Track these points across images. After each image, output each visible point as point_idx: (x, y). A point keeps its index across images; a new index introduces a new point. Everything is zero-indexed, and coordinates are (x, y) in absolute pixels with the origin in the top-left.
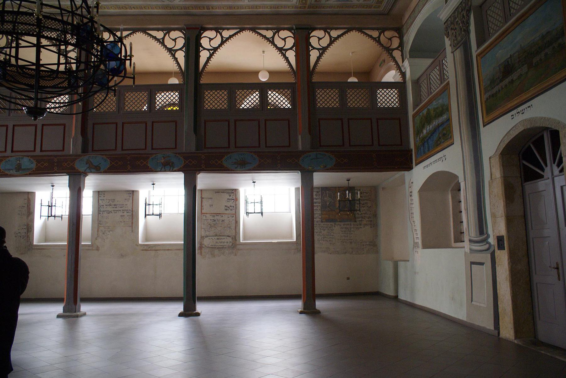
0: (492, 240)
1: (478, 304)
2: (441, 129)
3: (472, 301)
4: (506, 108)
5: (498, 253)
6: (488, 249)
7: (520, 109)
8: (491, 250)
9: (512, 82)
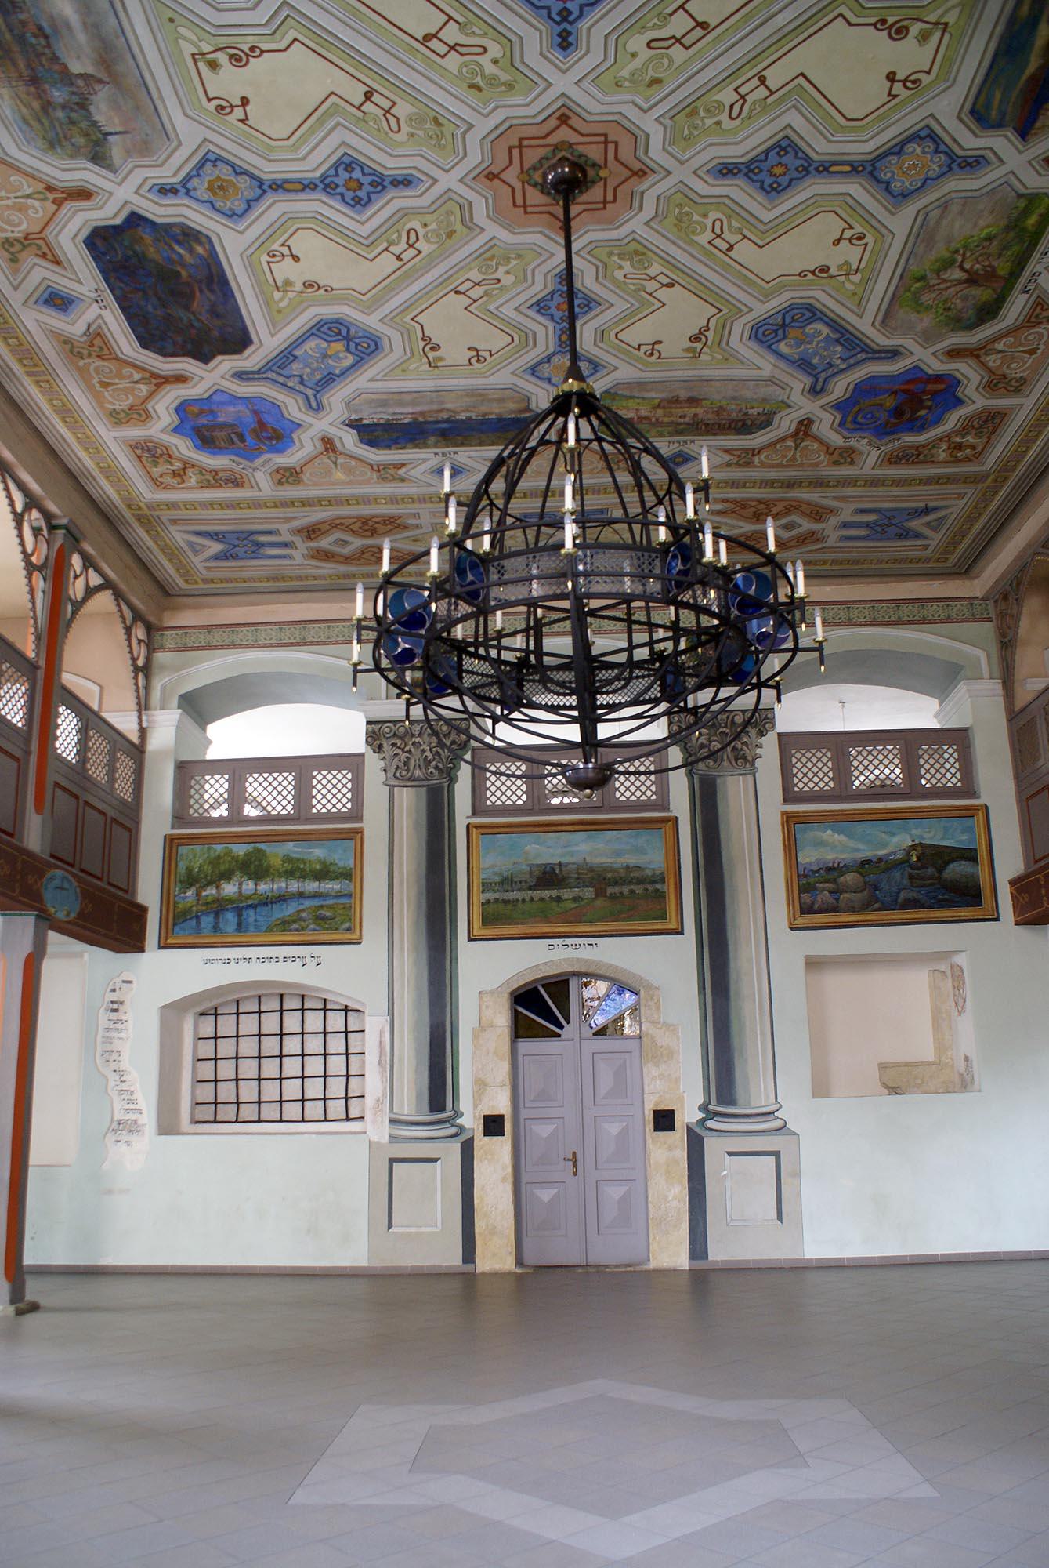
0: (470, 1120)
1: (413, 1230)
2: (308, 903)
3: (390, 1226)
4: (533, 930)
5: (482, 1142)
6: (456, 1135)
7: (568, 941)
8: (464, 1137)
9: (559, 899)
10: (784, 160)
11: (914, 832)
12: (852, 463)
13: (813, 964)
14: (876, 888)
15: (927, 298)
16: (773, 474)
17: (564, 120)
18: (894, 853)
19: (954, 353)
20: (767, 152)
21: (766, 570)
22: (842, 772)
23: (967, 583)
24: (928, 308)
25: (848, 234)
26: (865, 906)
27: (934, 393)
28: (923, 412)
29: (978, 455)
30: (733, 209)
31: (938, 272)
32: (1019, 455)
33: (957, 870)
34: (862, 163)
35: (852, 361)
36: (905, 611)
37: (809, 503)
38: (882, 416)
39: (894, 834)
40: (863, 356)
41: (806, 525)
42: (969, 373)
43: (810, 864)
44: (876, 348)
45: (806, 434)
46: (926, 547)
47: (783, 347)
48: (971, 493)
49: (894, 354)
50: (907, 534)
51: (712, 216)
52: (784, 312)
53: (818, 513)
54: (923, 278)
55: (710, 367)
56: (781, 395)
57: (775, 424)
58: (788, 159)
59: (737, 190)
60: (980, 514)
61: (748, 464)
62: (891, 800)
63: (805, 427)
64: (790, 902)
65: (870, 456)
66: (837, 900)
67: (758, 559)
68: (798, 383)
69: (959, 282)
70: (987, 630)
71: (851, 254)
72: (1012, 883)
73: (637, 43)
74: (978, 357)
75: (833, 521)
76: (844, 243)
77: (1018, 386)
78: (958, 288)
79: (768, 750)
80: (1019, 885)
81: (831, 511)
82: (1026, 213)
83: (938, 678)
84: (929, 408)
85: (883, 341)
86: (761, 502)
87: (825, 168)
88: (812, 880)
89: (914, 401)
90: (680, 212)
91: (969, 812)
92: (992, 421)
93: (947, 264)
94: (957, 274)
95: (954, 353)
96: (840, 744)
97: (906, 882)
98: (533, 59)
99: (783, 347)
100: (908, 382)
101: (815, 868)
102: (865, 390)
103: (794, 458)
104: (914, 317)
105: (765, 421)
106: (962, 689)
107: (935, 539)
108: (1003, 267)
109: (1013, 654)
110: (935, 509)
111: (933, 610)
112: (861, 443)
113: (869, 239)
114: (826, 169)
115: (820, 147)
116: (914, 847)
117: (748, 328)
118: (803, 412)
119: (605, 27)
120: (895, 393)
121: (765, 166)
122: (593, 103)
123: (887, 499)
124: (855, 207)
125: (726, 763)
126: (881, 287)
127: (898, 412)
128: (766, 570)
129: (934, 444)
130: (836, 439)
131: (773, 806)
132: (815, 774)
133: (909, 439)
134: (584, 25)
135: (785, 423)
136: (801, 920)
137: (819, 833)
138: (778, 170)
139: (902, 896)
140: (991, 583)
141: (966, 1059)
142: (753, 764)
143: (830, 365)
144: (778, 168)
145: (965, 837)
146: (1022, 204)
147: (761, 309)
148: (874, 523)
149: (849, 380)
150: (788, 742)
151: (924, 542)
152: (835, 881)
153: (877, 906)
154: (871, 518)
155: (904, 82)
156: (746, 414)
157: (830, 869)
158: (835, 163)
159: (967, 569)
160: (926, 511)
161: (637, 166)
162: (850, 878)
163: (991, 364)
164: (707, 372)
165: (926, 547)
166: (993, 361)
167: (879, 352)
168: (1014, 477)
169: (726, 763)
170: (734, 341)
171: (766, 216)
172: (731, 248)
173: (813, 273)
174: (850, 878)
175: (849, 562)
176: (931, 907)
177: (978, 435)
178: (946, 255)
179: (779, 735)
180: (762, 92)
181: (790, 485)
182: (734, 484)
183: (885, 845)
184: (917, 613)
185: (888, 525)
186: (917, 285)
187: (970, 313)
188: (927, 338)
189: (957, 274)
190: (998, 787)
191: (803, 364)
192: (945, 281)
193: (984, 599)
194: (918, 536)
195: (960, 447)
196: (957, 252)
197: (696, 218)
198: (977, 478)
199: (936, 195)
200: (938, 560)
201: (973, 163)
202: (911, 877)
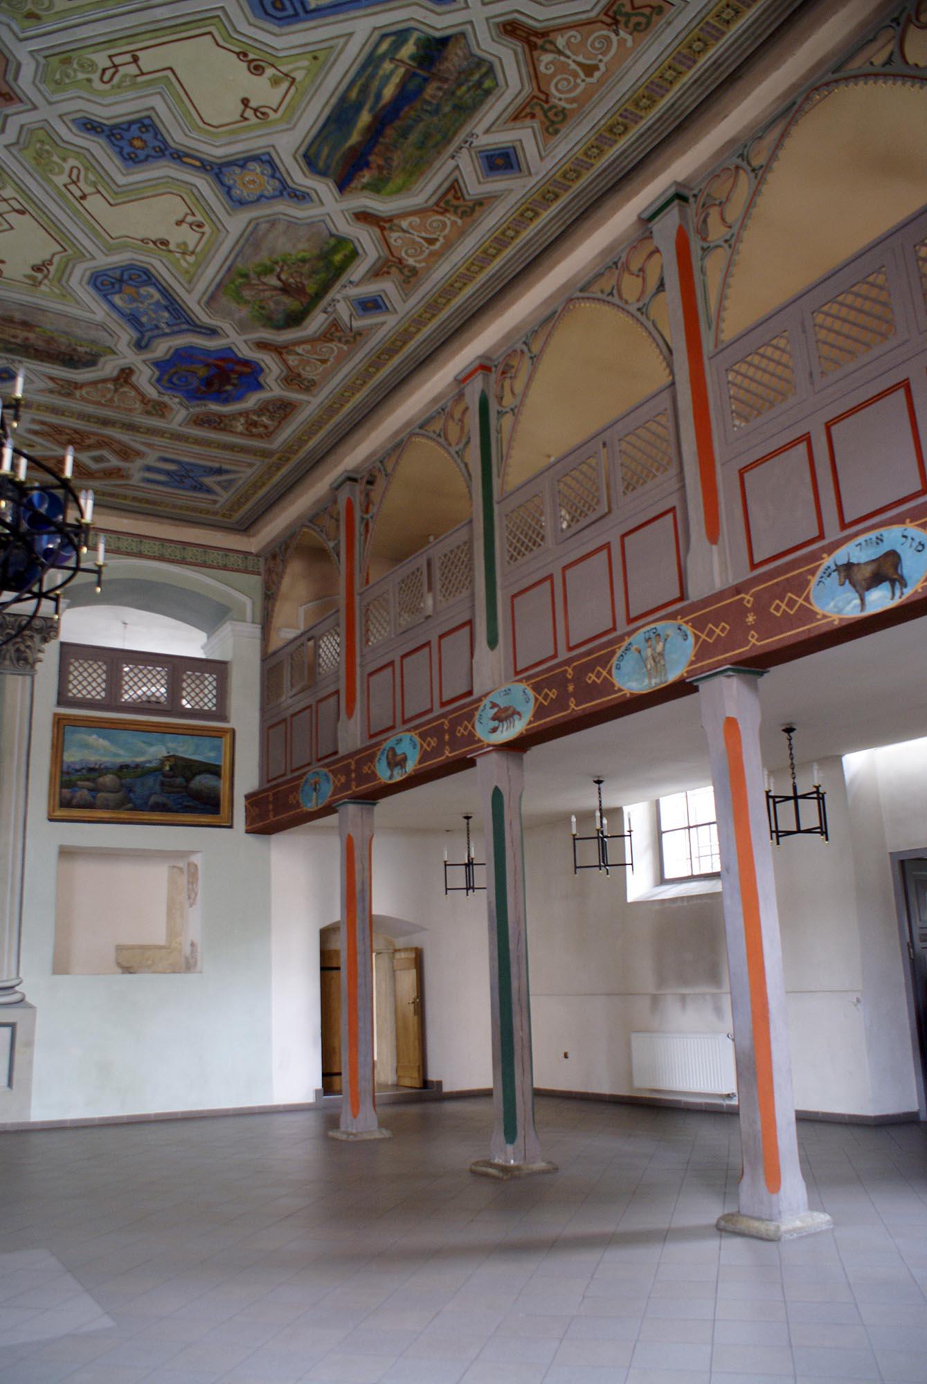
10: (144, 136)
11: (170, 745)
12: (163, 416)
13: (66, 853)
14: (131, 791)
15: (247, 294)
16: (91, 409)
18: (150, 762)
19: (262, 345)
20: (131, 123)
21: (60, 493)
22: (114, 683)
23: (245, 539)
24: (247, 302)
25: (190, 219)
26: (119, 806)
27: (241, 374)
28: (229, 388)
29: (269, 435)
30: (92, 164)
31: (259, 275)
32: (301, 442)
33: (202, 781)
34: (211, 164)
35: (176, 328)
36: (189, 553)
37: (119, 442)
38: (195, 383)
39: (151, 745)
40: (184, 327)
41: (114, 462)
42: (271, 366)
43: (74, 763)
44: (198, 322)
45: (126, 381)
46: (215, 502)
47: (117, 299)
48: (259, 464)
49: (212, 332)
50: (200, 488)
51: (72, 162)
52: (124, 269)
53: (126, 453)
54: (246, 276)
55: (45, 297)
56: (109, 342)
57: (100, 365)
58: (148, 137)
59: (97, 147)
60: (264, 484)
61: (69, 395)
62: (130, 712)
63: (125, 375)
64: (51, 795)
65: (179, 414)
66: (94, 797)
67: (56, 482)
68: (125, 336)
69: (275, 288)
70: (255, 581)
71: (191, 238)
72: (247, 797)
74: (281, 354)
75: (139, 463)
76: (185, 226)
77: (310, 387)
78: (274, 293)
79: (49, 655)
80: (253, 800)
81: (139, 454)
82: (334, 250)
83: (208, 615)
84: (234, 385)
85: (204, 318)
86: (76, 431)
87: (179, 156)
88: (74, 778)
89: (222, 377)
91: (218, 734)
92: (284, 409)
93: (268, 271)
94: (274, 282)
95: (262, 345)
96: (114, 659)
97: (157, 788)
99: (117, 299)
100: (222, 359)
101: (78, 767)
102: (183, 356)
103: (111, 400)
104: (234, 306)
105: (91, 361)
106: (227, 629)
107: (224, 497)
108: (311, 288)
109: (273, 605)
110: (227, 472)
111: (214, 557)
112: (173, 401)
113: (207, 229)
114: (179, 158)
115: (177, 137)
116: (168, 758)
117: (88, 274)
118: (127, 361)
120: (208, 365)
123: (188, 454)
124: (199, 198)
125: (7, 662)
126: (210, 273)
127: (208, 382)
128: (60, 493)
129: (234, 416)
130: (152, 393)
131: (46, 707)
132: (89, 682)
133: (214, 407)
135: (108, 367)
136: (59, 813)
137: (85, 737)
138: (137, 143)
139: (153, 799)
140: (264, 543)
141: (192, 945)
142: (33, 666)
143: (157, 327)
144: (138, 141)
145: (212, 754)
146: (332, 241)
147: (104, 261)
148: (174, 472)
149: (171, 343)
150: (70, 652)
151: (215, 498)
152: (94, 780)
153: (130, 805)
154: (172, 467)
155: (256, 110)
156: (75, 350)
157: (91, 770)
158: (188, 156)
159: (247, 527)
160: (219, 471)
162: (108, 779)
163: (290, 363)
164: (44, 303)
165: (215, 502)
166: (292, 360)
167: (201, 327)
168: (295, 459)
169: (7, 662)
170: (74, 282)
171: (121, 180)
172: (84, 197)
173: (154, 243)
174: (108, 779)
175: (147, 502)
176: (177, 811)
177: (271, 418)
178: (269, 263)
179: (62, 644)
181: (106, 422)
182: (55, 410)
183: (143, 753)
184: (201, 558)
185: (185, 477)
186: (241, 280)
187: (279, 317)
188: (242, 327)
189: (274, 282)
190: (245, 716)
191: (133, 320)
193: (258, 555)
194: (209, 491)
195: (255, 424)
196: (277, 263)
197: (55, 158)
198: (265, 454)
199: (267, 211)
200: (224, 516)
201: (300, 197)
202: (162, 784)
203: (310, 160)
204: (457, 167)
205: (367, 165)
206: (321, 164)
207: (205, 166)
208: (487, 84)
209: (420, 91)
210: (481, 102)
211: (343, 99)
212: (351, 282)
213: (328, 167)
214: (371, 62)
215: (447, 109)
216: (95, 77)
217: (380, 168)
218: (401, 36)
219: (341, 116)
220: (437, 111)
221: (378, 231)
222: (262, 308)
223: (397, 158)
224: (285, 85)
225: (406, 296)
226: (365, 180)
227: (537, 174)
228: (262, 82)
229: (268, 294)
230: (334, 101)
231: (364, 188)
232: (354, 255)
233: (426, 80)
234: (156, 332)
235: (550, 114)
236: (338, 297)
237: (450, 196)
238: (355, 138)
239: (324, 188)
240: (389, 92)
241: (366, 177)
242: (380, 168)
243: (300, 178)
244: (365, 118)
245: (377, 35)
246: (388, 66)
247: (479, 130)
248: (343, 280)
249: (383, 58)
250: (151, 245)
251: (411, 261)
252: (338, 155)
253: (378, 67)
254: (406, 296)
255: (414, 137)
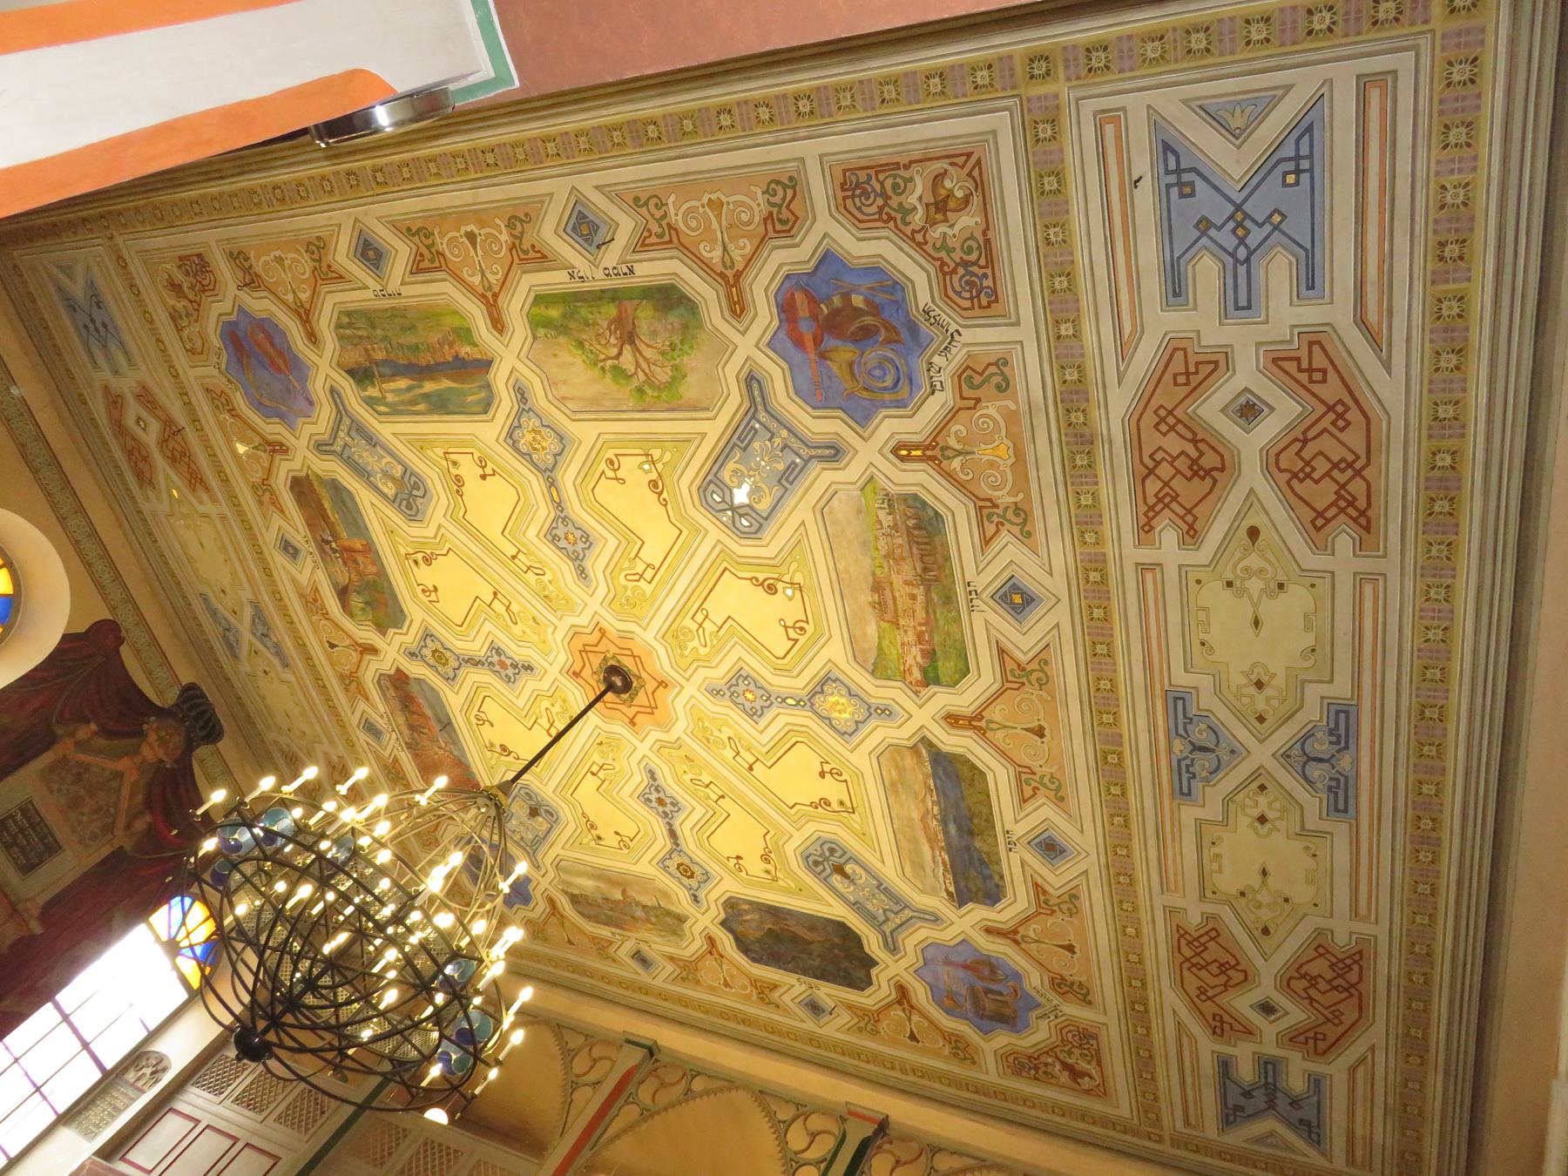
17: (577, 675)
25: (610, 474)
30: (611, 569)
44: (746, 404)
54: (640, 390)
58: (560, 532)
59: (597, 564)
73: (517, 630)
76: (620, 474)
78: (643, 347)
87: (559, 506)
90: (628, 606)
93: (618, 372)
98: (545, 684)
113: (610, 454)
114: (559, 505)
115: (544, 513)
119: (514, 647)
121: (570, 548)
122: (563, 658)
134: (517, 658)
144: (570, 539)
149: (807, 419)
161: (597, 634)
163: (748, 250)
167: (752, 399)
173: (660, 494)
180: (521, 556)
186: (649, 391)
187: (674, 318)
192: (638, 365)
196: (603, 369)
199: (554, 411)
201: (522, 394)
203: (486, 406)
204: (402, 284)
205: (456, 357)
206: (483, 395)
207: (552, 484)
208: (345, 320)
209: (385, 362)
210: (356, 311)
211: (430, 412)
212: (572, 276)
213: (480, 387)
214: (395, 411)
215: (379, 332)
216: (545, 579)
217: (451, 345)
218: (370, 402)
219: (441, 405)
220: (385, 338)
221: (500, 300)
222: (673, 347)
223: (434, 338)
224: (453, 457)
225: (543, 200)
226: (468, 349)
227: (349, 215)
228: (461, 471)
229: (648, 353)
230: (436, 418)
231: (476, 345)
232: (540, 300)
233: (377, 364)
234: (796, 445)
235: (316, 256)
236: (599, 274)
237: (426, 264)
238: (446, 384)
239: (499, 377)
240: (402, 383)
241: (465, 350)
242: (451, 345)
243: (506, 403)
244: (429, 387)
245: (382, 418)
246: (390, 398)
247: (369, 294)
248: (577, 286)
249: (386, 405)
250: (665, 495)
251: (504, 237)
252: (465, 386)
253: (394, 404)
254: (543, 200)
255: (410, 339)
